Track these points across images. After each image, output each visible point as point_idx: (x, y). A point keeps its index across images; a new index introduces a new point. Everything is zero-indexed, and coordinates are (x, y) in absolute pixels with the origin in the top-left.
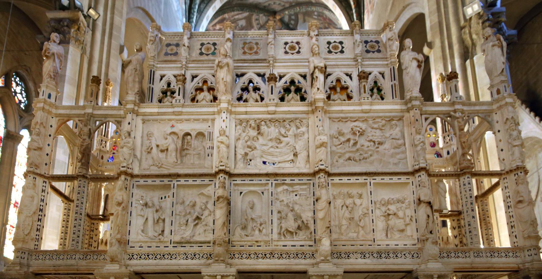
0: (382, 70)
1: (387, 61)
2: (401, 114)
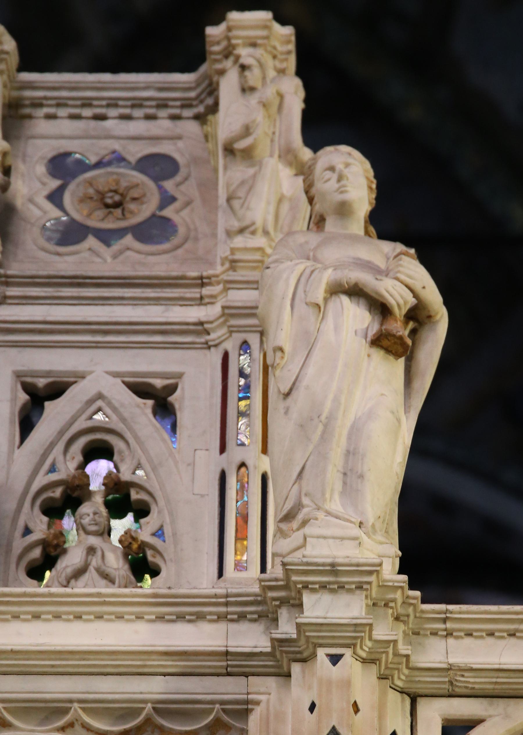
0: (153, 363)
1: (201, 301)
2: (230, 688)
